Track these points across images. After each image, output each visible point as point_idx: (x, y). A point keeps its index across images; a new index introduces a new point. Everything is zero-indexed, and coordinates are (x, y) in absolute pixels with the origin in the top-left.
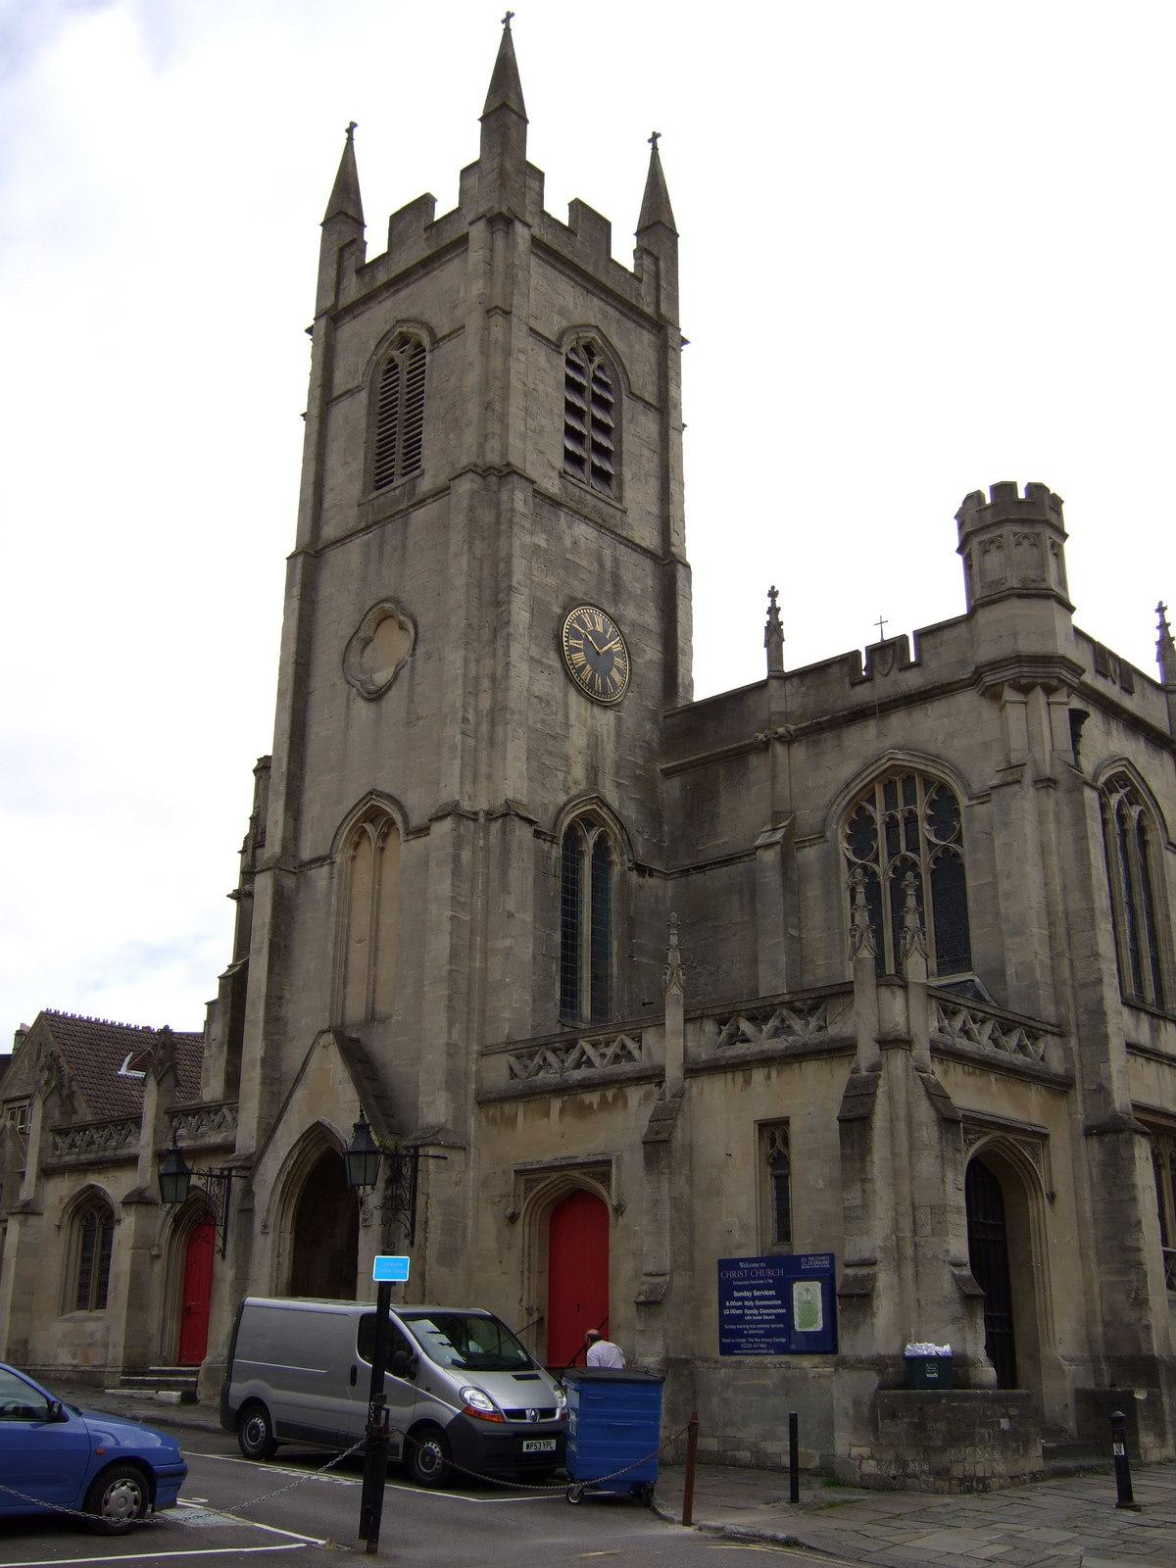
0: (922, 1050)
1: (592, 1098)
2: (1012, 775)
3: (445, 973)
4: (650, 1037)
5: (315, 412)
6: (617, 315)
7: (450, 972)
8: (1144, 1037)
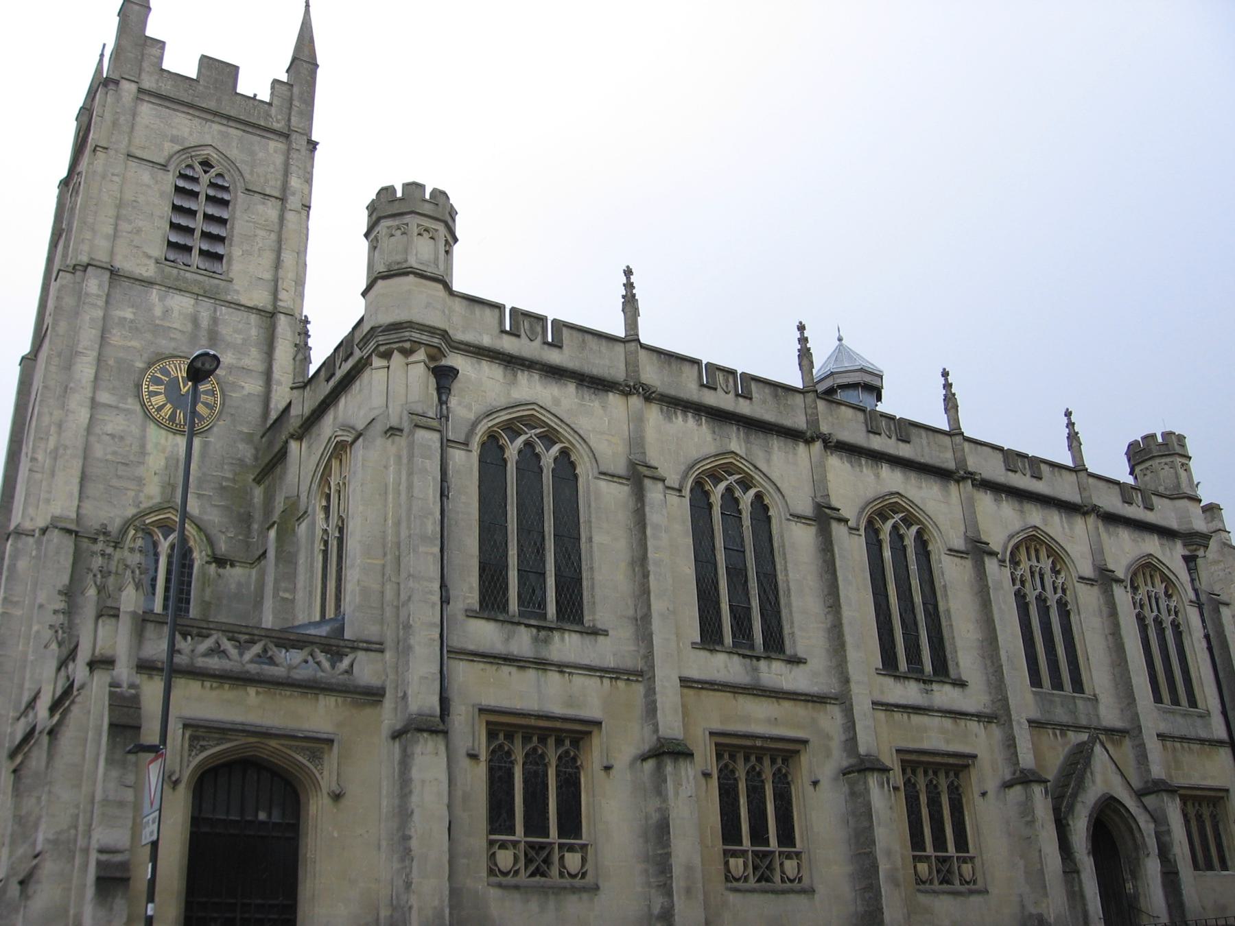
6: (239, 133)
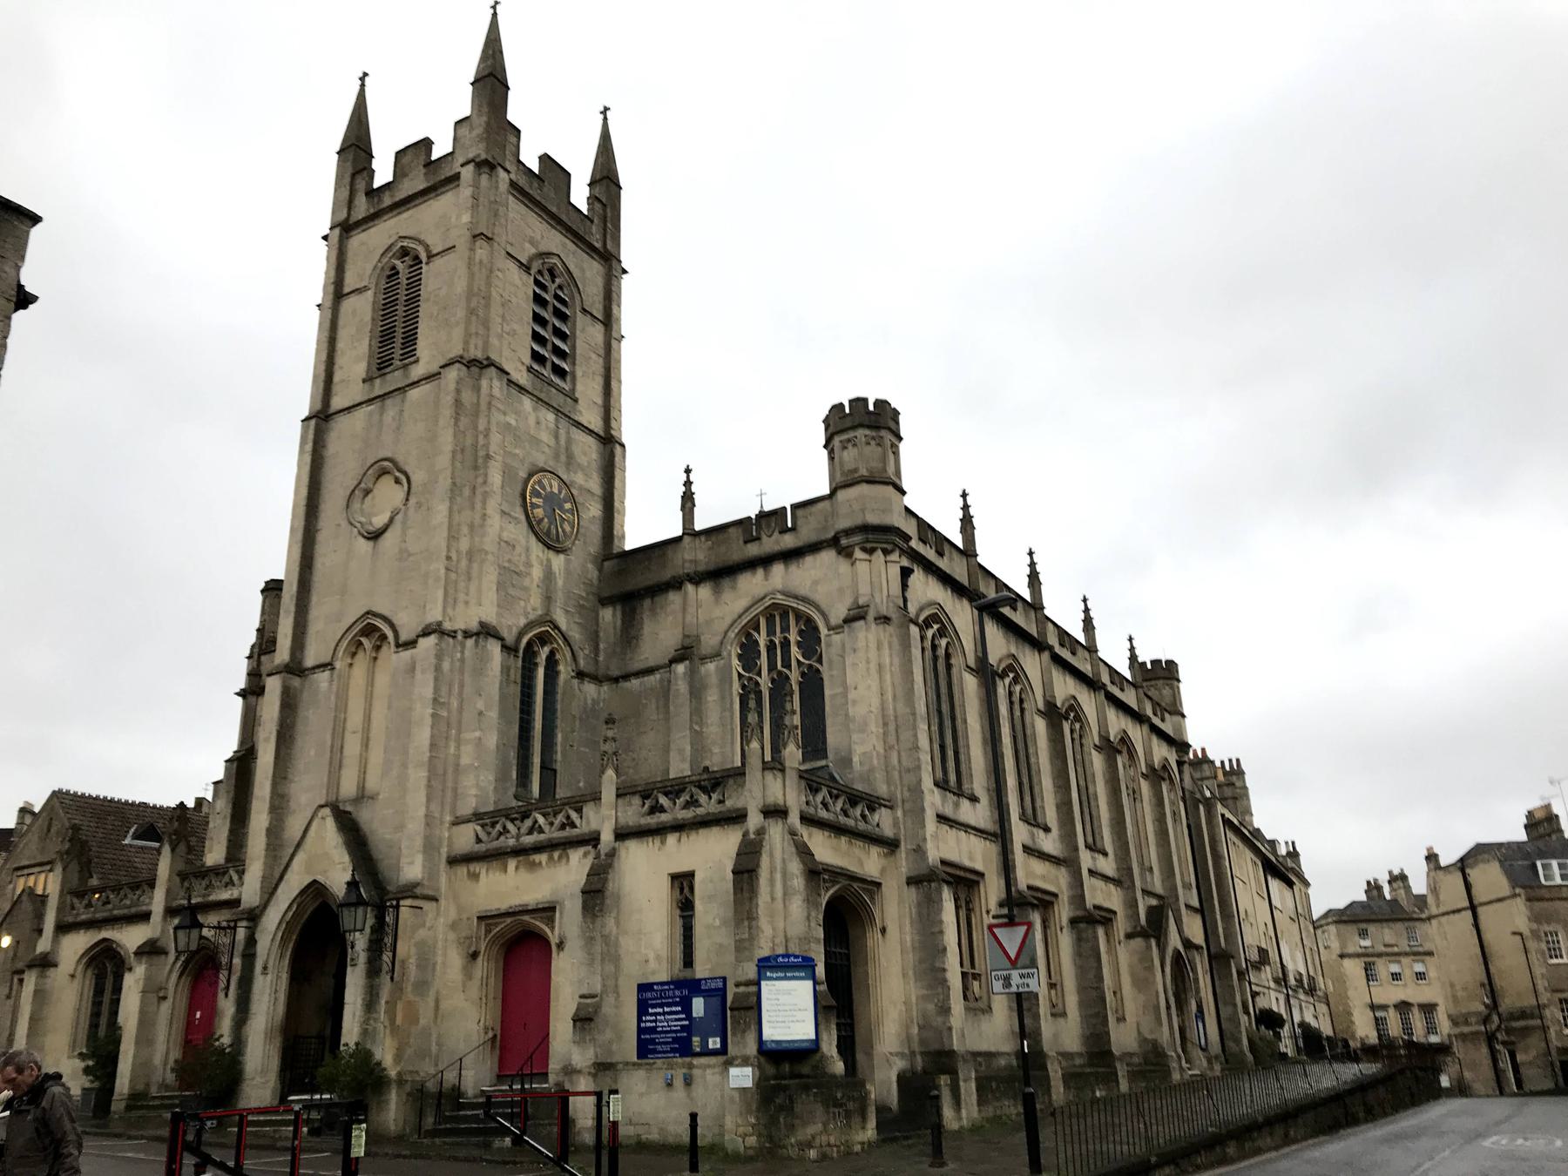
0: (793, 818)
1: (542, 858)
2: (857, 615)
3: (426, 759)
4: (588, 809)
5: (329, 304)
7: (431, 758)
8: (948, 811)
